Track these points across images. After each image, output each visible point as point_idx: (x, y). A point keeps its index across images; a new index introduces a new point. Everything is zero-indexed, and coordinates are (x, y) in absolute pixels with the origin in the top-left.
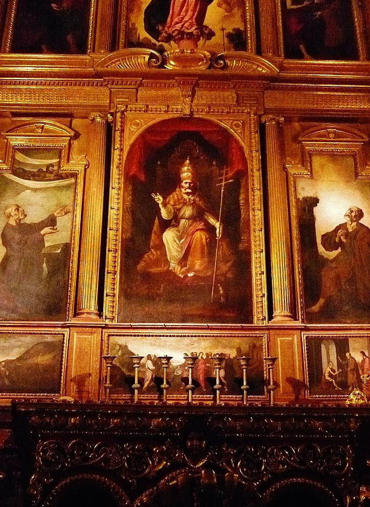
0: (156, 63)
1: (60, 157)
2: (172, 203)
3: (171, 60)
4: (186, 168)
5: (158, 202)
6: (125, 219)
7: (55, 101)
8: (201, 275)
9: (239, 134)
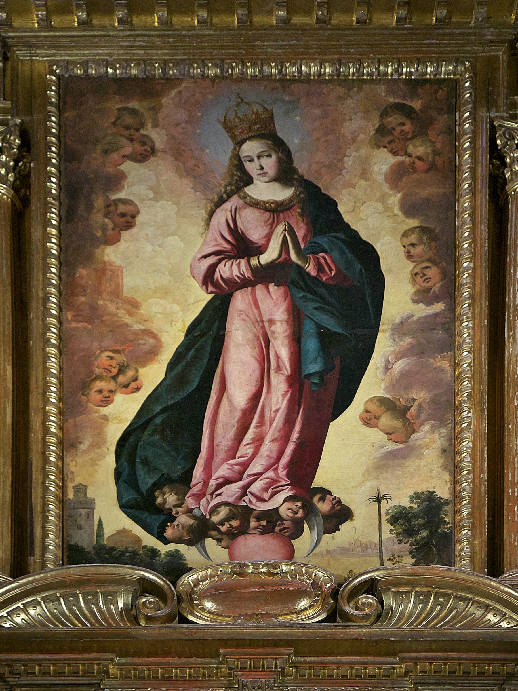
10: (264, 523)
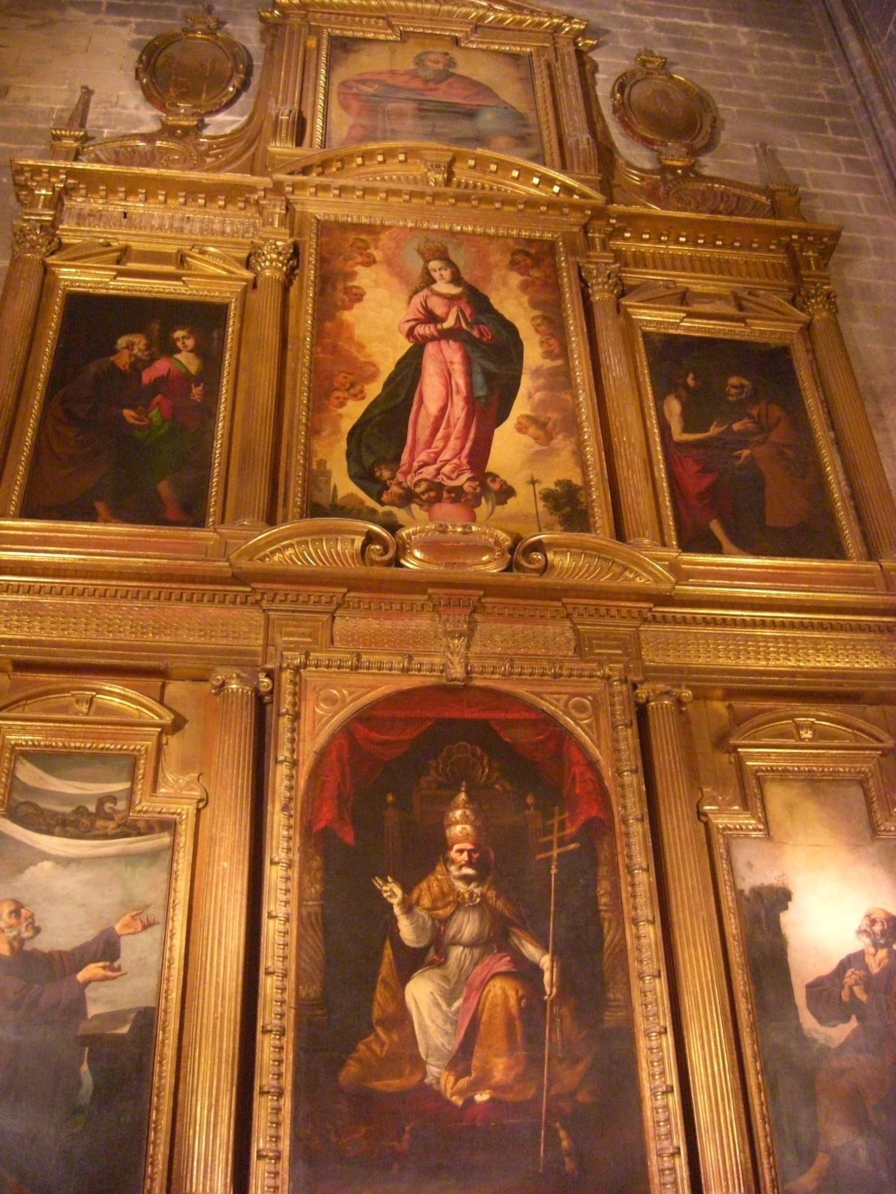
0: (382, 555)
1: (133, 778)
2: (426, 902)
3: (417, 548)
4: (458, 813)
5: (392, 901)
6: (304, 945)
7: (126, 637)
8: (510, 1097)
9: (586, 728)
10: (453, 495)
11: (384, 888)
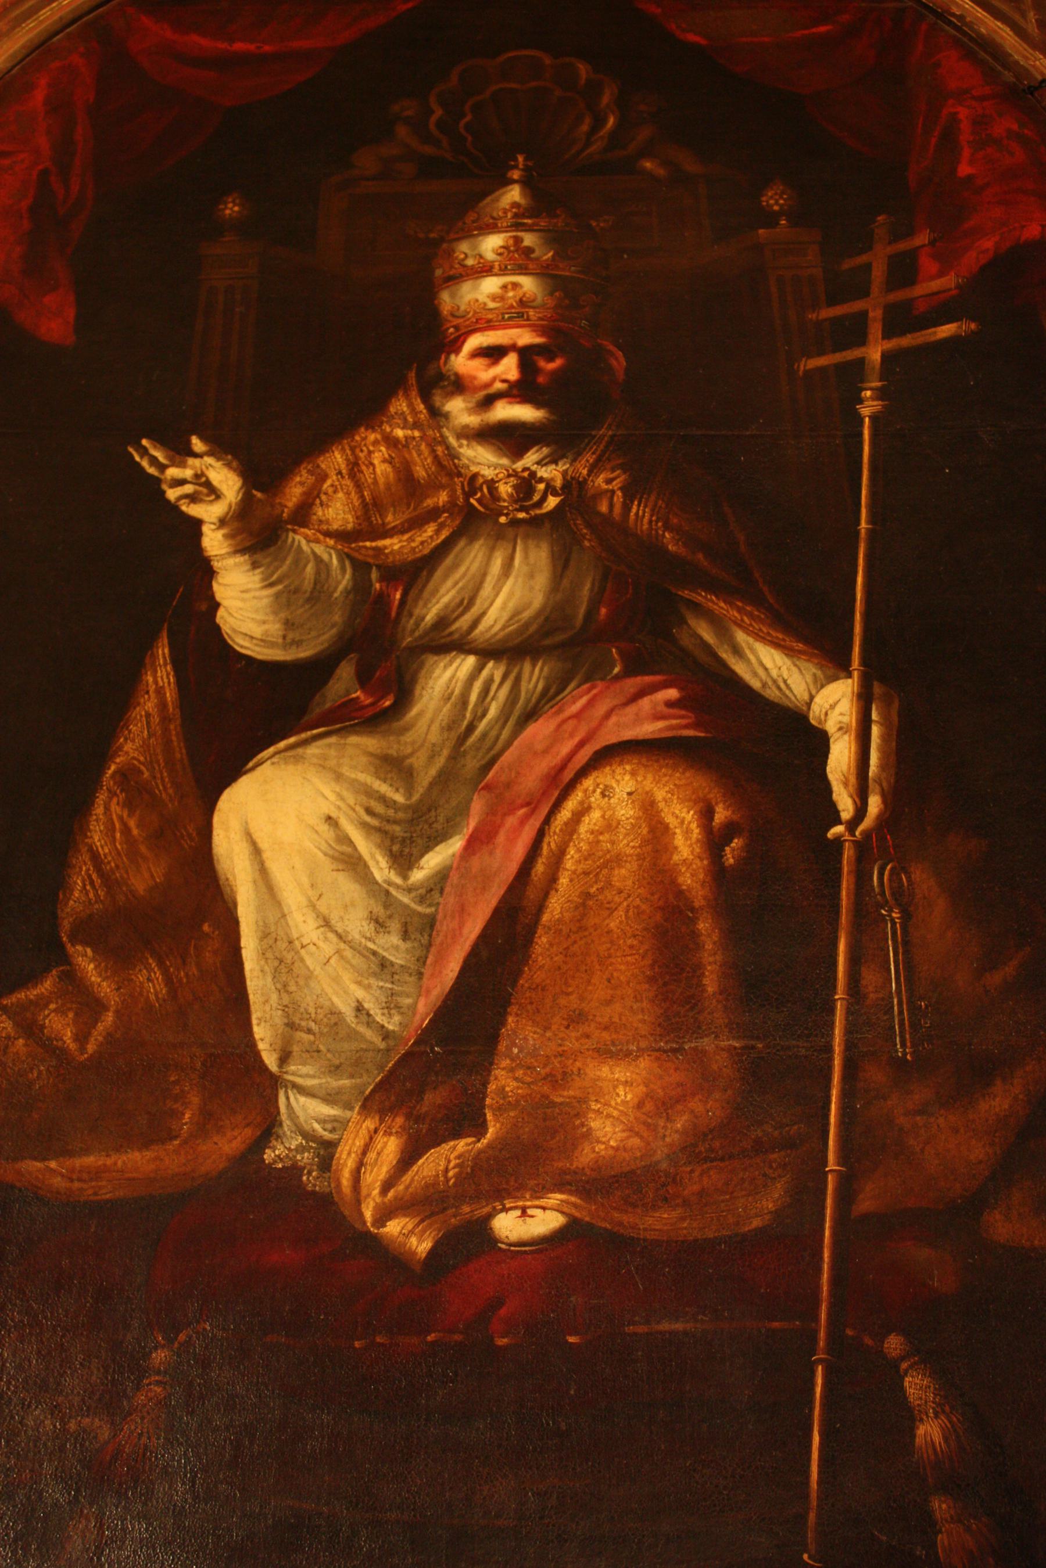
4: (491, 244)
5: (194, 510)
11: (173, 472)
